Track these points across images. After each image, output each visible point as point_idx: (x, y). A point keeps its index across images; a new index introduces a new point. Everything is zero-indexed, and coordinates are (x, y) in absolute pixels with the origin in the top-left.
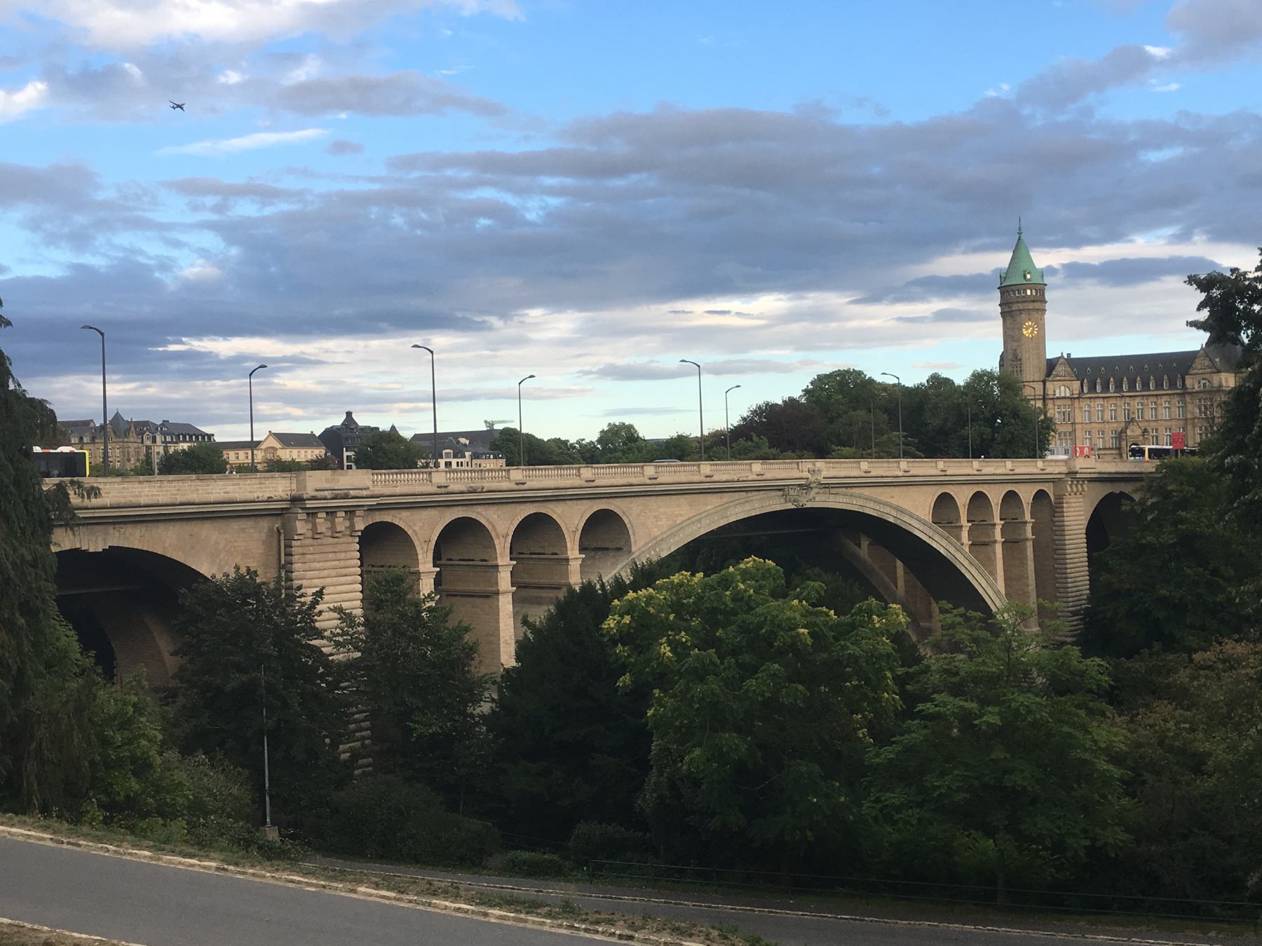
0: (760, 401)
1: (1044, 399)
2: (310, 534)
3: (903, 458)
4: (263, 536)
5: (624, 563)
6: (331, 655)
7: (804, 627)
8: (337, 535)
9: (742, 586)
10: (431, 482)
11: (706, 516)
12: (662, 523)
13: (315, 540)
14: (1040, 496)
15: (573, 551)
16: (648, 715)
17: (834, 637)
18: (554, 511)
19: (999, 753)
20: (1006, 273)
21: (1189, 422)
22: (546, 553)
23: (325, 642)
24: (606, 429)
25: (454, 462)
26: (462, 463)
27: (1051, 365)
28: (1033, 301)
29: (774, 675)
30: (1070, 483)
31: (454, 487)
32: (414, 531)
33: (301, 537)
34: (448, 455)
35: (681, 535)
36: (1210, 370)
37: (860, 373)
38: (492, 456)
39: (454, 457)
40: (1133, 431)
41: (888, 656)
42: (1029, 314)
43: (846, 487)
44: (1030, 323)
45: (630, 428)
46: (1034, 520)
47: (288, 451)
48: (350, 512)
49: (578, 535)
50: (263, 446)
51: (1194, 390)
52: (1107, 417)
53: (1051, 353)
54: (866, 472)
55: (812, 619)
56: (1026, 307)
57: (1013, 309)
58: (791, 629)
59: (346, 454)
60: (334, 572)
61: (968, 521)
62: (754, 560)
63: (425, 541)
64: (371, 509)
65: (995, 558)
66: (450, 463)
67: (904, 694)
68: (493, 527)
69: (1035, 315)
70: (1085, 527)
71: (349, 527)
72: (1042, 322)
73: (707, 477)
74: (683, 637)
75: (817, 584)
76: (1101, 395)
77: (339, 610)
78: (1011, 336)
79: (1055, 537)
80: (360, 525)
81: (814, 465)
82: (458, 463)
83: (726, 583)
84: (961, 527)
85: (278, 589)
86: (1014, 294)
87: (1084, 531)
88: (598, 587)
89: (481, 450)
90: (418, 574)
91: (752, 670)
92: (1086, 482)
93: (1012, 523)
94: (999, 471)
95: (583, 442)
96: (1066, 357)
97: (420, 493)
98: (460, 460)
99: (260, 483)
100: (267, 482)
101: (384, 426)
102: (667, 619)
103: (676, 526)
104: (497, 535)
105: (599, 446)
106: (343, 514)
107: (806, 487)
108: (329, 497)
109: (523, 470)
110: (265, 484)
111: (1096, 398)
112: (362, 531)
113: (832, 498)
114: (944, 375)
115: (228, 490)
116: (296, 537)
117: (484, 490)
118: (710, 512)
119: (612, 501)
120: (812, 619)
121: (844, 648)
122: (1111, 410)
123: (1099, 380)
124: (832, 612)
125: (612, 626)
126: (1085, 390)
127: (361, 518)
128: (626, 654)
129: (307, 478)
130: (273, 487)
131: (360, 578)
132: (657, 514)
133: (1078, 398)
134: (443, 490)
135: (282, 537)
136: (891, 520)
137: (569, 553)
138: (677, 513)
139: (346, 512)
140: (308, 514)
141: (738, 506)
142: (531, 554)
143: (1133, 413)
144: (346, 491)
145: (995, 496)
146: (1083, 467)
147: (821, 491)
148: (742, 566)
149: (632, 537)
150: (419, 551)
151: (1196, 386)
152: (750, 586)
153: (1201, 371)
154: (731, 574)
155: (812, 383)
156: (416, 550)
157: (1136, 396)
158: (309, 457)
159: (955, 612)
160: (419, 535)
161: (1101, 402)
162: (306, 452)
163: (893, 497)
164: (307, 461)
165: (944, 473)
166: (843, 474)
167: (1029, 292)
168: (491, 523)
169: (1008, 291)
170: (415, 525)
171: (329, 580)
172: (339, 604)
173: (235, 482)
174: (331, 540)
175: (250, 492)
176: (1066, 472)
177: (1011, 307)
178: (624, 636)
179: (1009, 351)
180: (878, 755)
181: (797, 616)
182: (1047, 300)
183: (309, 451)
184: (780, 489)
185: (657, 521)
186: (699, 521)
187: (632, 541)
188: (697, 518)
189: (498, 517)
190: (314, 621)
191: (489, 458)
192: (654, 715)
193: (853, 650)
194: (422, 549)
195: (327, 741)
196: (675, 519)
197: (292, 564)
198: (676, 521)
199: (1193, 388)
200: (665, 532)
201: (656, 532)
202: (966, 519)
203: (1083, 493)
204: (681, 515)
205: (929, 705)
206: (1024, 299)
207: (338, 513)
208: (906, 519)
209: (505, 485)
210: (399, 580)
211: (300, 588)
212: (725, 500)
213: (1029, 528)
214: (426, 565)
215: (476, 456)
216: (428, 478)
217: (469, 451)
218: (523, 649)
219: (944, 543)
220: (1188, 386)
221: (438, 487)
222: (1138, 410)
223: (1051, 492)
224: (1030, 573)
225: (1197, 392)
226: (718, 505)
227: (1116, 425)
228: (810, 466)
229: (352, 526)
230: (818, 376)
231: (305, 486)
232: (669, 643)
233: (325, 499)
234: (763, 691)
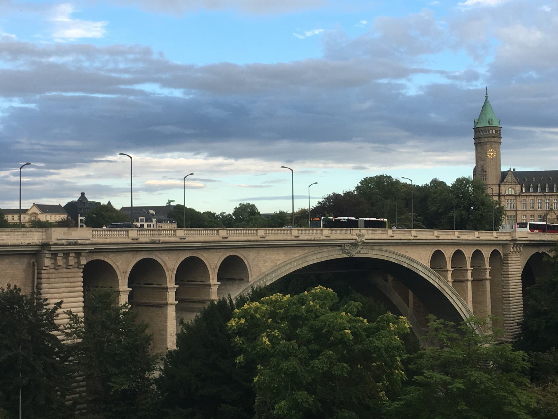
0: (331, 193)
1: (499, 196)
2: (52, 266)
3: (414, 228)
4: (24, 267)
5: (244, 288)
6: (63, 340)
7: (350, 329)
8: (69, 267)
9: (312, 303)
10: (128, 236)
11: (294, 261)
12: (268, 264)
13: (55, 270)
14: (495, 254)
15: (213, 280)
16: (255, 381)
17: (366, 335)
18: (160, 258)
19: (463, 406)
20: (479, 120)
22: (197, 280)
23: (60, 333)
24: (238, 207)
25: (146, 224)
26: (150, 225)
27: (504, 175)
28: (494, 137)
29: (329, 357)
30: (512, 246)
31: (142, 240)
32: (117, 266)
33: (47, 268)
34: (142, 220)
35: (279, 272)
37: (390, 177)
38: (169, 222)
39: (146, 221)
40: (551, 216)
41: (398, 348)
42: (491, 145)
43: (379, 245)
44: (492, 150)
45: (253, 206)
46: (491, 268)
47: (44, 215)
48: (78, 254)
49: (217, 270)
50: (30, 212)
52: (536, 207)
53: (504, 169)
54: (391, 237)
55: (354, 324)
56: (489, 141)
57: (482, 141)
58: (341, 330)
59: (80, 218)
60: (67, 290)
61: (452, 268)
62: (321, 288)
63: (123, 272)
64: (91, 252)
65: (468, 291)
66: (143, 225)
67: (407, 371)
68: (165, 264)
69: (495, 145)
70: (521, 272)
71: (77, 262)
72: (499, 149)
73: (295, 237)
74: (276, 333)
75: (357, 303)
76: (532, 194)
77: (69, 313)
78: (480, 158)
79: (503, 278)
80: (84, 262)
81: (360, 231)
82: (148, 225)
83: (303, 302)
84: (448, 271)
85: (32, 300)
86: (483, 132)
87: (521, 275)
88: (228, 301)
89: (162, 217)
90: (118, 292)
91: (315, 355)
92: (522, 246)
93: (477, 269)
94: (470, 238)
95: (224, 214)
96: (512, 170)
97: (121, 243)
98: (149, 224)
99: (23, 235)
100: (27, 234)
101: (104, 202)
102: (267, 321)
103: (276, 267)
104: (168, 270)
105: (234, 217)
106: (74, 255)
107: (355, 245)
108: (65, 244)
109: (184, 230)
110: (26, 235)
111: (530, 195)
112: (85, 265)
113: (370, 252)
114: (440, 179)
115: (3, 238)
116: (44, 268)
117: (160, 242)
118: (298, 258)
119: (238, 250)
120: (354, 324)
121: (371, 342)
122: (539, 203)
123: (531, 185)
124: (366, 320)
125: (234, 324)
126: (524, 191)
127: (85, 257)
128: (241, 342)
129: (52, 232)
130: (31, 237)
131: (82, 294)
132: (265, 259)
133: (519, 195)
134: (135, 241)
135: (36, 268)
136: (406, 265)
137: (211, 281)
138: (277, 258)
139: (75, 253)
140: (52, 254)
141: (314, 255)
142: (188, 281)
143: (552, 205)
144: (76, 241)
145: (468, 253)
146: (521, 236)
147: (364, 247)
148: (313, 291)
149: (249, 272)
150: (120, 278)
152: (317, 303)
154: (305, 296)
155: (360, 183)
156: (118, 278)
157: (553, 195)
158: (57, 219)
159: (438, 321)
160: (120, 268)
161: (532, 198)
162: (55, 216)
163: (407, 252)
164: (56, 222)
165: (438, 238)
166: (377, 237)
167: (491, 131)
168: (164, 262)
169: (479, 131)
170: (117, 262)
171: (64, 295)
172: (69, 309)
173: (8, 233)
174: (65, 270)
175: (17, 240)
176: (511, 239)
177: (481, 140)
178: (240, 331)
179: (479, 166)
180: (389, 406)
181: (345, 322)
183: (57, 216)
184: (340, 245)
185: (265, 263)
186: (290, 263)
187: (250, 275)
188: (290, 261)
189: (169, 258)
190: (53, 320)
191: (167, 222)
192: (258, 380)
193: (377, 343)
194: (121, 276)
195: (59, 393)
196: (276, 262)
197: (41, 284)
198: (276, 264)
200: (269, 270)
201: (264, 269)
202: (450, 266)
203: (520, 252)
204: (279, 260)
205: (421, 377)
207: (70, 254)
208: (415, 265)
209: (173, 239)
210: (108, 295)
211: (46, 300)
212: (306, 251)
213: (488, 272)
214: (124, 287)
215: (159, 221)
216: (126, 234)
217: (155, 218)
218: (180, 338)
219: (437, 280)
221: (133, 239)
222: (554, 203)
223: (501, 251)
224: (488, 300)
226: (302, 254)
227: (541, 212)
228: (358, 232)
229: (78, 263)
230: (365, 180)
231: (51, 237)
232: (268, 336)
233: (63, 245)
234: (323, 367)
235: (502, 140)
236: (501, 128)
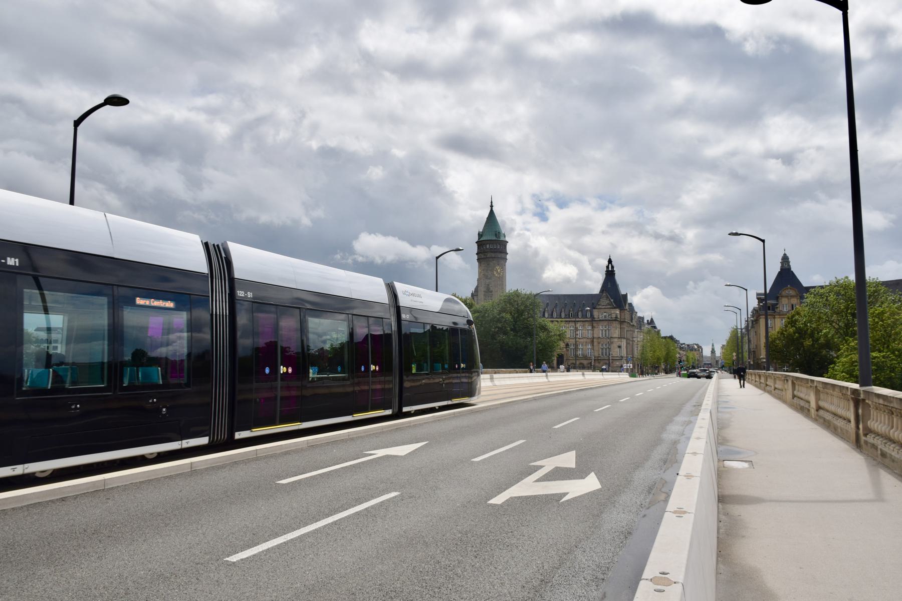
20: (482, 232)
21: (595, 340)
36: (609, 307)
51: (599, 319)
56: (496, 256)
57: (488, 256)
151: (600, 317)
153: (603, 307)
177: (487, 256)
182: (508, 252)
199: (599, 318)
206: (495, 251)
220: (595, 317)
225: (600, 320)
235: (508, 257)
236: (508, 242)
